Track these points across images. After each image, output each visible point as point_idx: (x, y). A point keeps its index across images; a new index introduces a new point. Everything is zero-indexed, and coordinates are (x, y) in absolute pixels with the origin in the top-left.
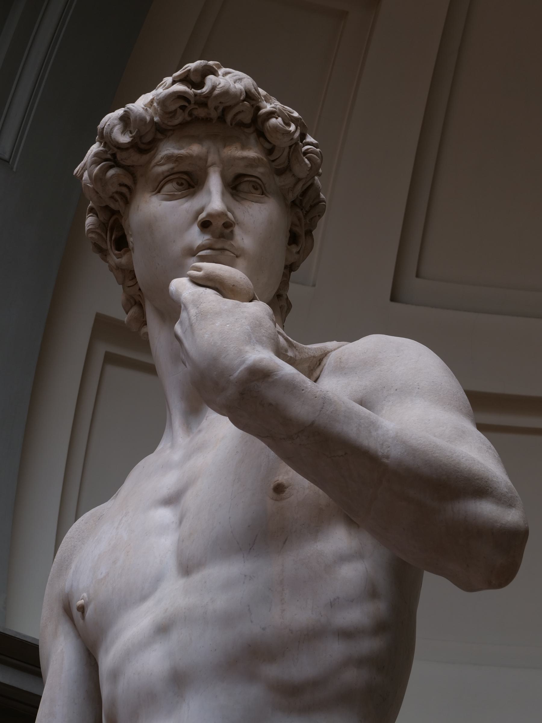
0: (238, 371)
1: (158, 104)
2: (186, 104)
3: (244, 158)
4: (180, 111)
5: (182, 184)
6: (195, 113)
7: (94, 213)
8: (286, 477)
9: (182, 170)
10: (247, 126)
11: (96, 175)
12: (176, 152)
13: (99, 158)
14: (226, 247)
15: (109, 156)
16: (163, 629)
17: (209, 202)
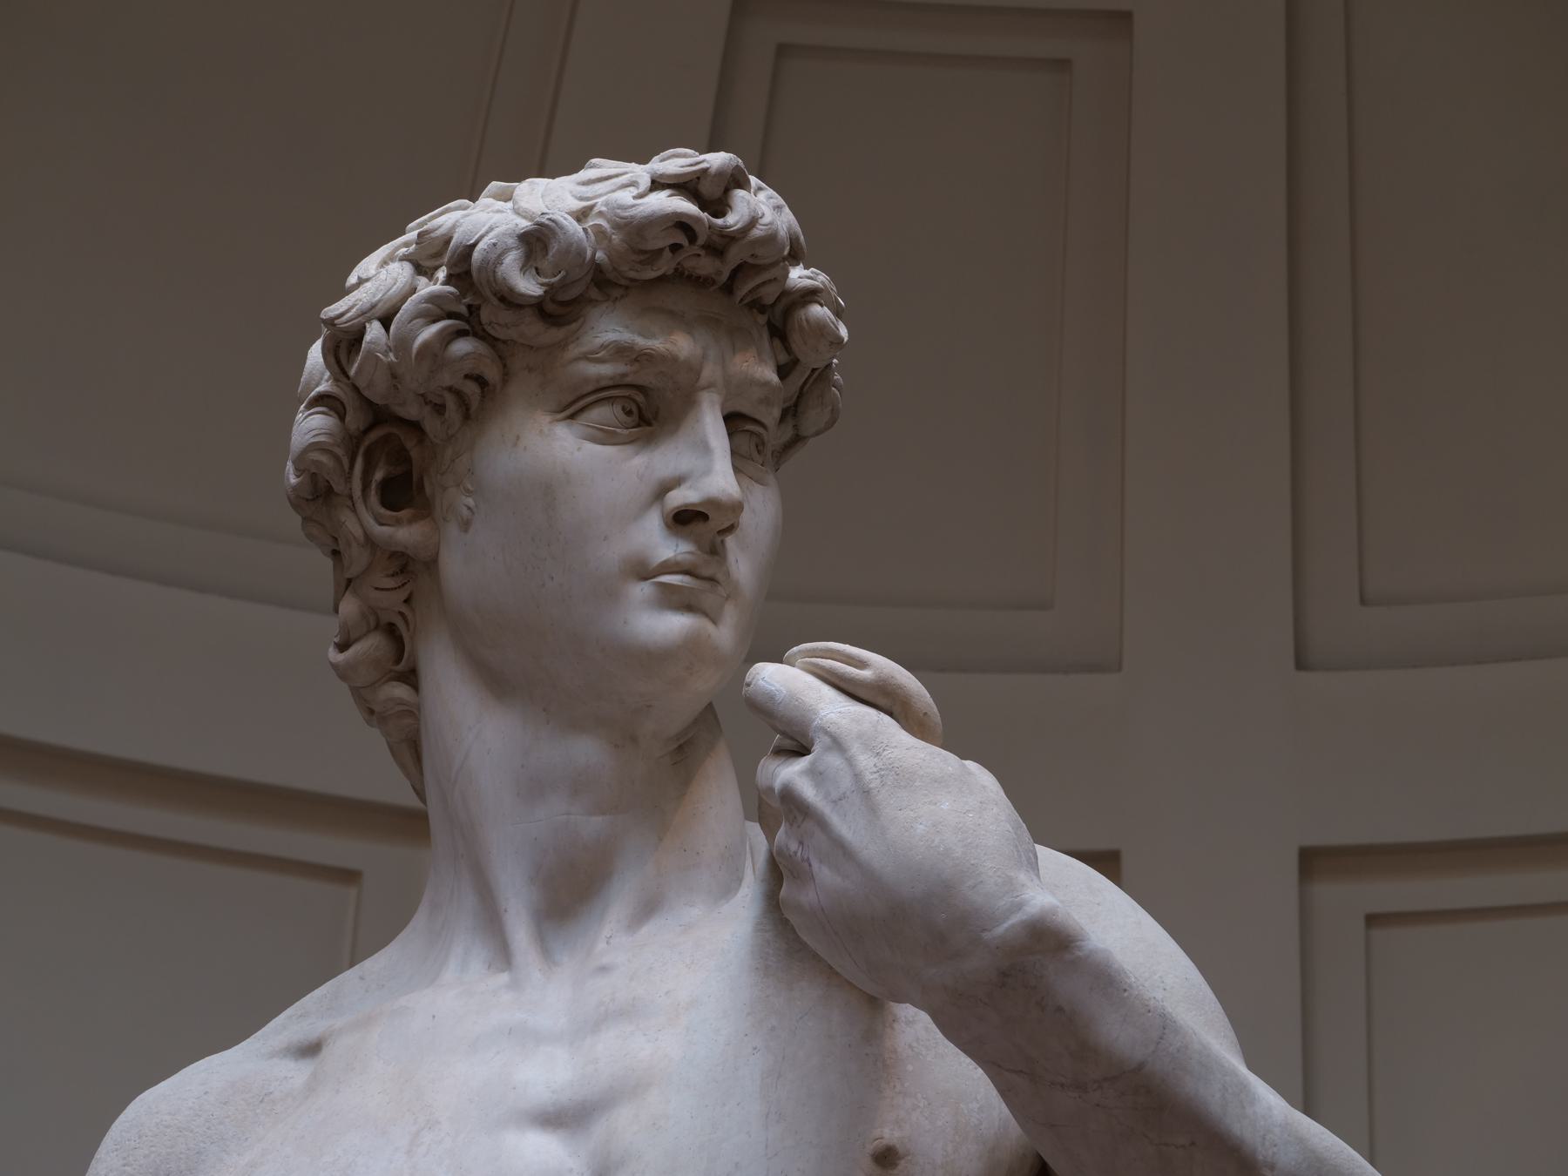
0: (1006, 925)
1: (617, 226)
2: (685, 242)
3: (766, 384)
4: (667, 254)
5: (629, 413)
6: (689, 264)
7: (331, 408)
8: (897, 1134)
9: (639, 382)
10: (762, 309)
11: (426, 346)
12: (641, 342)
13: (436, 309)
14: (720, 576)
15: (463, 310)
17: (708, 471)
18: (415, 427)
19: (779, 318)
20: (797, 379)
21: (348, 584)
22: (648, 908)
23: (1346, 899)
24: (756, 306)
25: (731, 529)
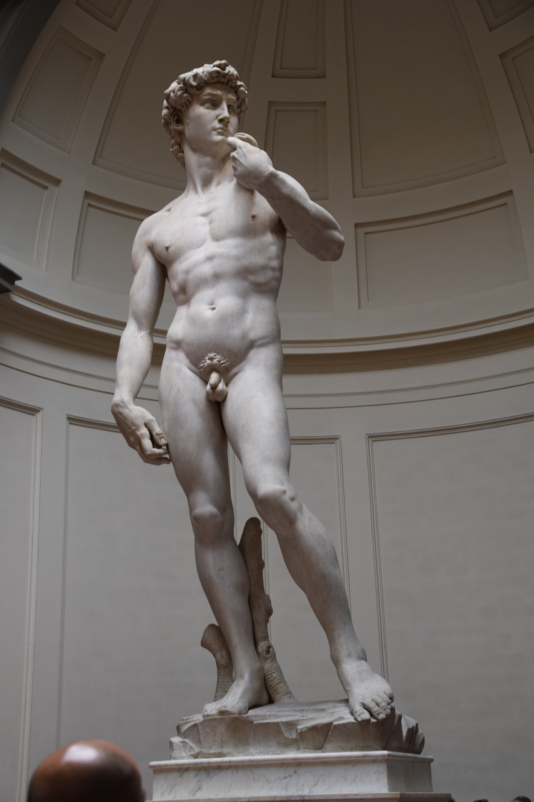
3: (233, 100)
4: (216, 78)
6: (220, 80)
10: (233, 88)
11: (179, 95)
12: (213, 92)
16: (210, 258)
17: (224, 113)
18: (180, 110)
19: (236, 90)
20: (240, 101)
21: (173, 138)
22: (219, 183)
23: (361, 231)
24: (232, 87)
25: (228, 122)
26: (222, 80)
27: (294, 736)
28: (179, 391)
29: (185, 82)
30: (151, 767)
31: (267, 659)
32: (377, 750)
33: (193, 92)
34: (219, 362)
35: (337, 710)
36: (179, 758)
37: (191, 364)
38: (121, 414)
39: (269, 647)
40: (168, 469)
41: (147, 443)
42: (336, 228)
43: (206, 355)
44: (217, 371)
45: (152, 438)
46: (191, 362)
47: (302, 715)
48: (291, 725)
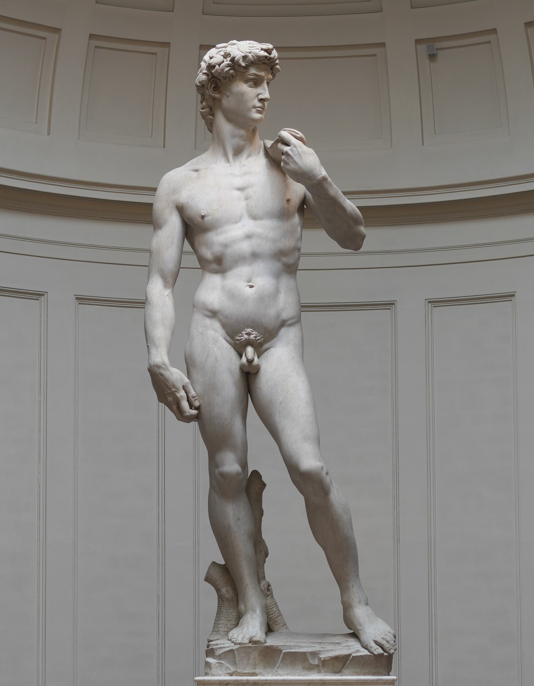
11: (226, 71)
12: (258, 73)
13: (228, 65)
16: (249, 237)
17: (265, 93)
22: (249, 156)
26: (267, 62)
27: (316, 662)
28: (216, 359)
29: (233, 60)
30: (195, 681)
31: (268, 596)
32: (385, 675)
33: (238, 69)
34: (251, 336)
35: (349, 644)
36: (217, 675)
37: (226, 335)
38: (162, 375)
39: (269, 585)
40: (194, 425)
41: (185, 405)
42: (361, 224)
43: (243, 329)
44: (252, 346)
45: (188, 401)
46: (227, 333)
47: (320, 646)
48: (314, 654)
